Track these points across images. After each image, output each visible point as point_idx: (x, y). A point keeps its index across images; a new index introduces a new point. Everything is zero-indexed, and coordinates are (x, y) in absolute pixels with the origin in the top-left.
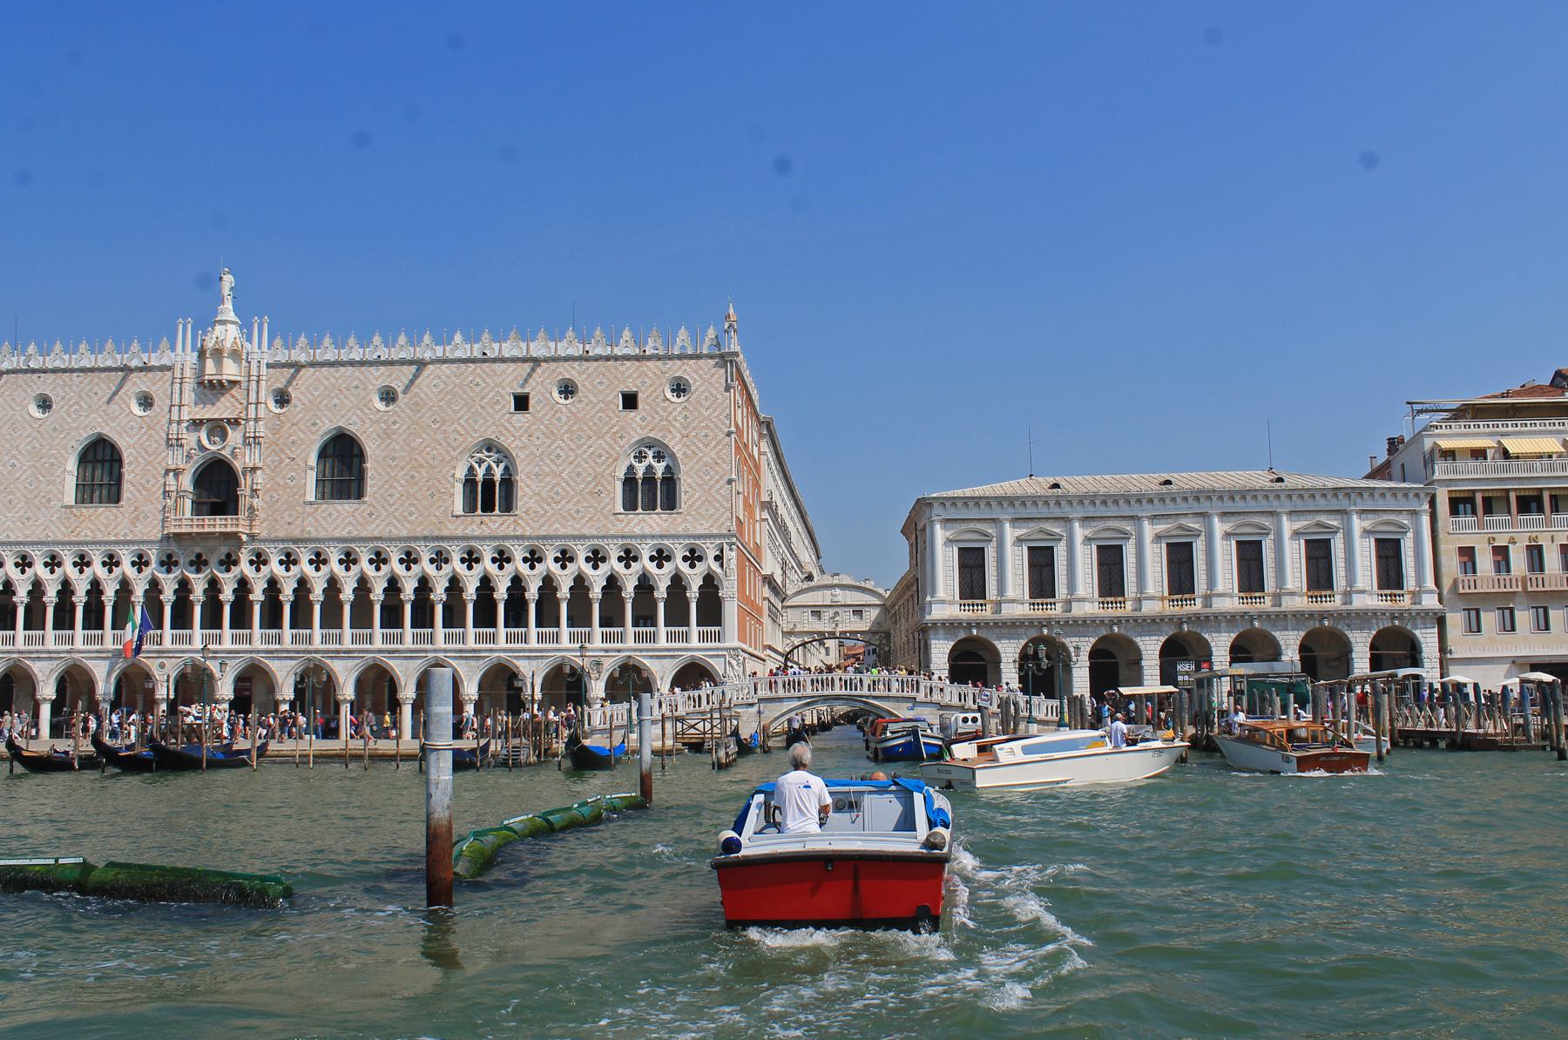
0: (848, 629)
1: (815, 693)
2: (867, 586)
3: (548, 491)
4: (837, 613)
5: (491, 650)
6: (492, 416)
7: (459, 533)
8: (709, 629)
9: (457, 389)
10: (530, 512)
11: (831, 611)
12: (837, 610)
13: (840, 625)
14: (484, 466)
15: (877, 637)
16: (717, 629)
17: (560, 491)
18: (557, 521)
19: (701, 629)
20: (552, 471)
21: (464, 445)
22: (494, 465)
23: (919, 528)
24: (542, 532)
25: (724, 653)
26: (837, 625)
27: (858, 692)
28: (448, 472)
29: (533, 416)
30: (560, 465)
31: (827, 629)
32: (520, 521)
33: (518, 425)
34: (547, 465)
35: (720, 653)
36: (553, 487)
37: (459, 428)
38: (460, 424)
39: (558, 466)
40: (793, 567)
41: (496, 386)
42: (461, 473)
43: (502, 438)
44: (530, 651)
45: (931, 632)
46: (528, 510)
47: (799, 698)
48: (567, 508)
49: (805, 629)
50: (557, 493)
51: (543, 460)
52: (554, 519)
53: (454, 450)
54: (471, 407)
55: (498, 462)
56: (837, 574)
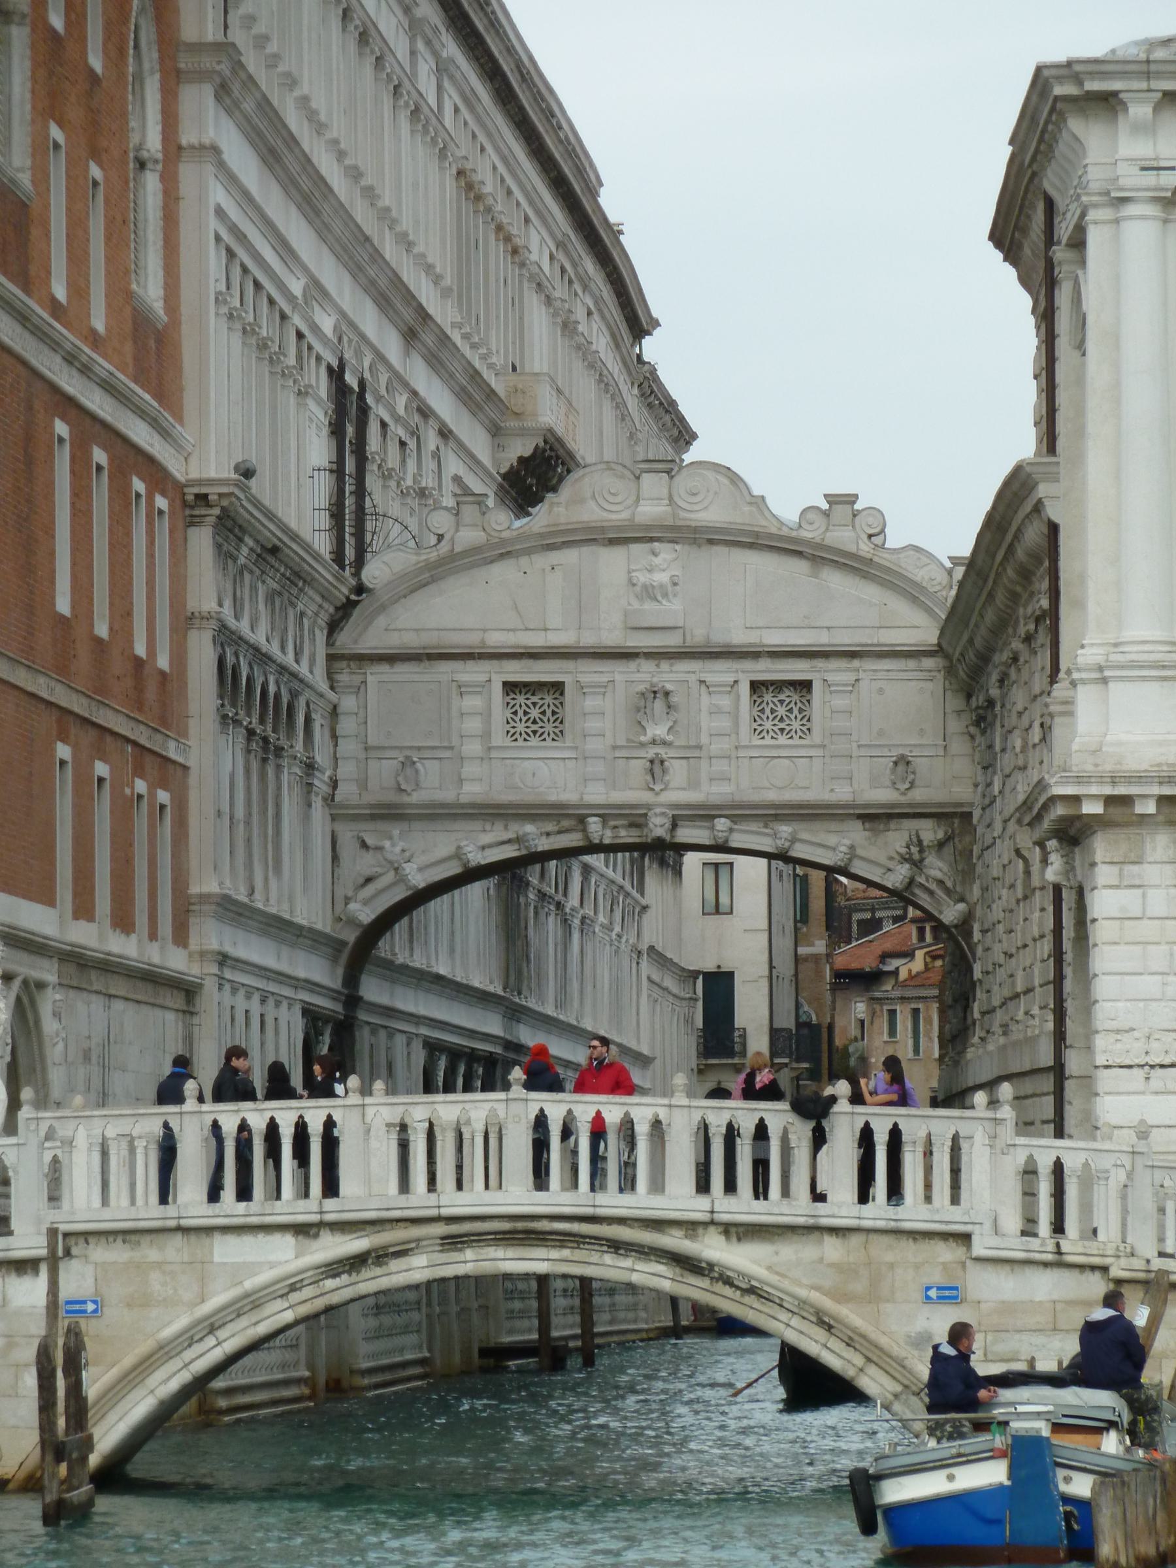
12: (670, 675)
13: (678, 771)
15: (897, 839)
23: (1064, 230)
26: (656, 767)
27: (641, 1202)
31: (596, 794)
40: (425, 412)
45: (1101, 846)
47: (302, 1230)
49: (472, 791)
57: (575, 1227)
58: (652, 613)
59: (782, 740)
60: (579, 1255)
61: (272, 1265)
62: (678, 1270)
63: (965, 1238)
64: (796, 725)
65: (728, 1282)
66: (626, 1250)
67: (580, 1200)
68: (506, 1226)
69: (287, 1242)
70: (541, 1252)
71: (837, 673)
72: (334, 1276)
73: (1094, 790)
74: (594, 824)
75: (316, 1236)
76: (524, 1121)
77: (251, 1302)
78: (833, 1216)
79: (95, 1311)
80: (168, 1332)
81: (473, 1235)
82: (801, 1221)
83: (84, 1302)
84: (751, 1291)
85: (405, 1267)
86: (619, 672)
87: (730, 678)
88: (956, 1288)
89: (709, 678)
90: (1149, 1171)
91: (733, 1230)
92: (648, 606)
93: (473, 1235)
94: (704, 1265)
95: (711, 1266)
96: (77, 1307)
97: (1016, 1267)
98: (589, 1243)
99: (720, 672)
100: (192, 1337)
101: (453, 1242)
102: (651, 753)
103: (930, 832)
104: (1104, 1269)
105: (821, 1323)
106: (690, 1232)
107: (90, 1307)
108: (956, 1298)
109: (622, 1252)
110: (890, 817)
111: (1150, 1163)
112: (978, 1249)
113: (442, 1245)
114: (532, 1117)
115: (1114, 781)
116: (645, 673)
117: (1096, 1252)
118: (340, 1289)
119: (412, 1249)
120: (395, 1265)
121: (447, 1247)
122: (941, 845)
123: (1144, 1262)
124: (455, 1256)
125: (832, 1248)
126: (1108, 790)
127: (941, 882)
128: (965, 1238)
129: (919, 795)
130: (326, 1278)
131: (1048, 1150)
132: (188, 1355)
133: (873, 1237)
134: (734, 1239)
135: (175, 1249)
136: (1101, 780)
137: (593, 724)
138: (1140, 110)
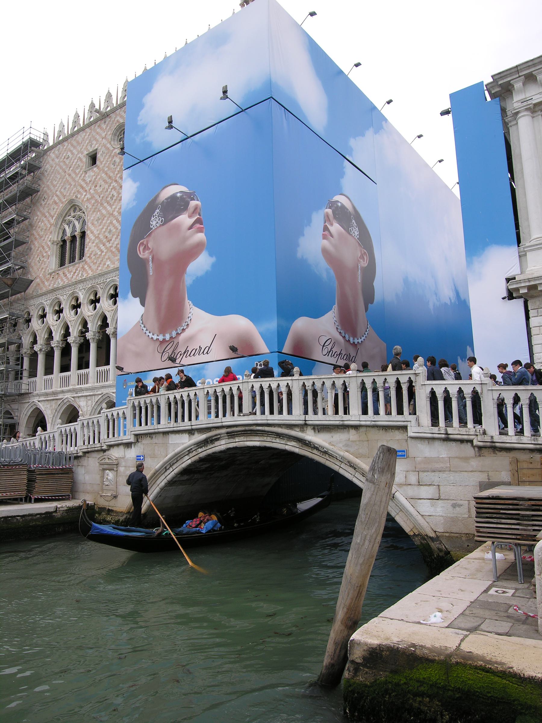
1: (213, 421)
3: (104, 232)
5: (63, 392)
6: (74, 180)
7: (51, 288)
9: (57, 167)
10: (92, 255)
14: (71, 226)
17: (112, 228)
18: (109, 258)
20: (108, 211)
21: (58, 210)
22: (76, 223)
24: (99, 272)
27: (285, 417)
28: (48, 238)
29: (98, 168)
30: (113, 205)
32: (86, 266)
33: (88, 180)
34: (105, 208)
36: (107, 229)
37: (56, 199)
38: (57, 196)
39: (111, 206)
41: (78, 154)
42: (56, 237)
43: (79, 196)
44: (87, 389)
46: (91, 254)
47: (191, 432)
48: (116, 243)
50: (110, 232)
51: (102, 204)
52: (107, 257)
53: (52, 218)
54: (64, 178)
55: (79, 219)
57: (267, 429)
60: (269, 439)
61: (183, 444)
62: (300, 444)
63: (405, 428)
65: (317, 449)
66: (283, 437)
67: (268, 418)
68: (243, 428)
69: (186, 436)
70: (257, 438)
72: (201, 447)
73: (523, 285)
75: (194, 434)
76: (248, 390)
77: (178, 457)
78: (349, 421)
79: (143, 459)
80: (157, 467)
81: (270, 432)
82: (337, 423)
83: (140, 456)
84: (326, 453)
85: (219, 444)
88: (404, 451)
90: (490, 392)
91: (316, 428)
93: (270, 432)
94: (307, 442)
95: (310, 442)
96: (139, 458)
97: (430, 441)
98: (271, 435)
100: (166, 468)
101: (231, 435)
104: (471, 441)
105: (351, 466)
106: (302, 429)
107: (142, 458)
108: (404, 456)
109: (281, 437)
111: (491, 388)
112: (410, 434)
113: (228, 436)
114: (250, 388)
115: (529, 280)
117: (465, 433)
118: (204, 452)
119: (219, 438)
120: (217, 443)
121: (230, 437)
123: (490, 438)
124: (232, 440)
125: (352, 435)
126: (527, 284)
128: (405, 428)
130: (197, 449)
131: (440, 386)
132: (167, 473)
133: (368, 429)
134: (317, 431)
135: (159, 439)
136: (524, 281)
138: (518, 85)
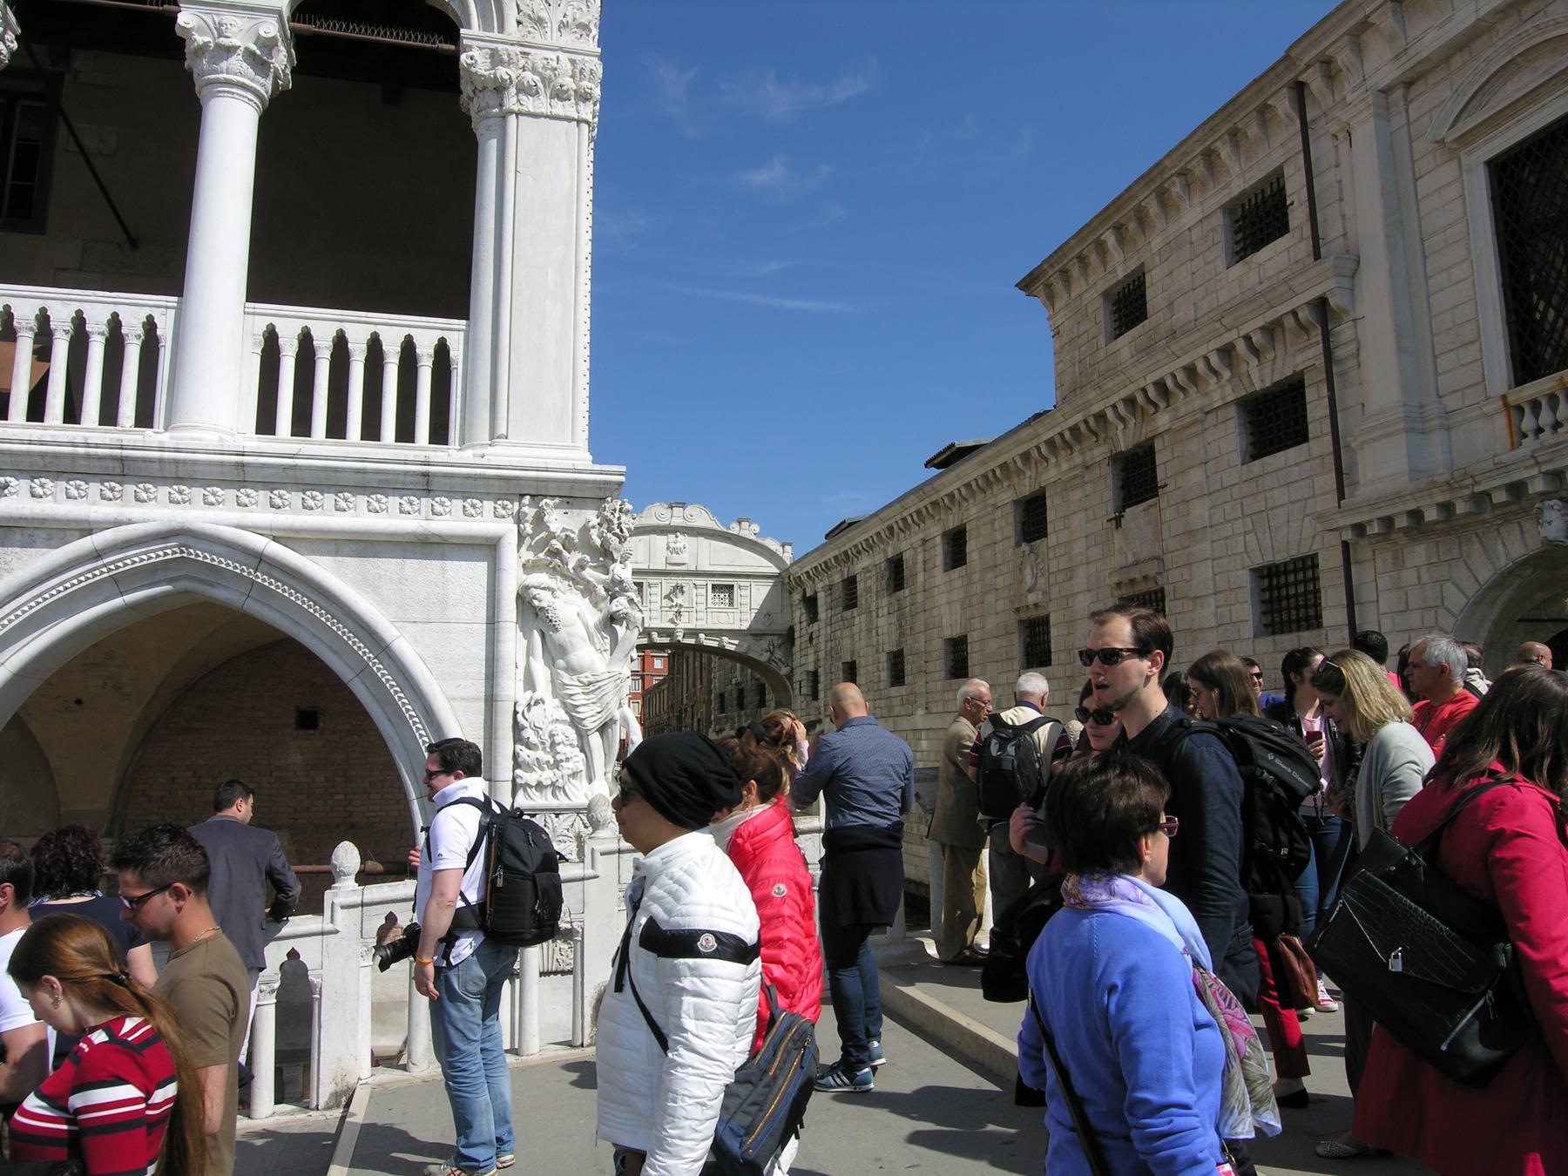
0: (701, 625)
2: (744, 533)
4: (679, 589)
8: (359, 327)
11: (667, 584)
12: (680, 581)
13: (685, 616)
15: (764, 644)
16: (426, 332)
19: (290, 321)
25: (486, 520)
26: (679, 613)
35: (452, 519)
56: (683, 505)
58: (676, 558)
59: (722, 606)
64: (727, 601)
71: (744, 582)
74: (655, 635)
86: (663, 580)
87: (705, 583)
89: (697, 583)
92: (675, 555)
99: (701, 581)
102: (676, 609)
103: (775, 639)
110: (762, 635)
116: (674, 581)
122: (780, 646)
127: (780, 660)
129: (773, 627)
137: (653, 598)
